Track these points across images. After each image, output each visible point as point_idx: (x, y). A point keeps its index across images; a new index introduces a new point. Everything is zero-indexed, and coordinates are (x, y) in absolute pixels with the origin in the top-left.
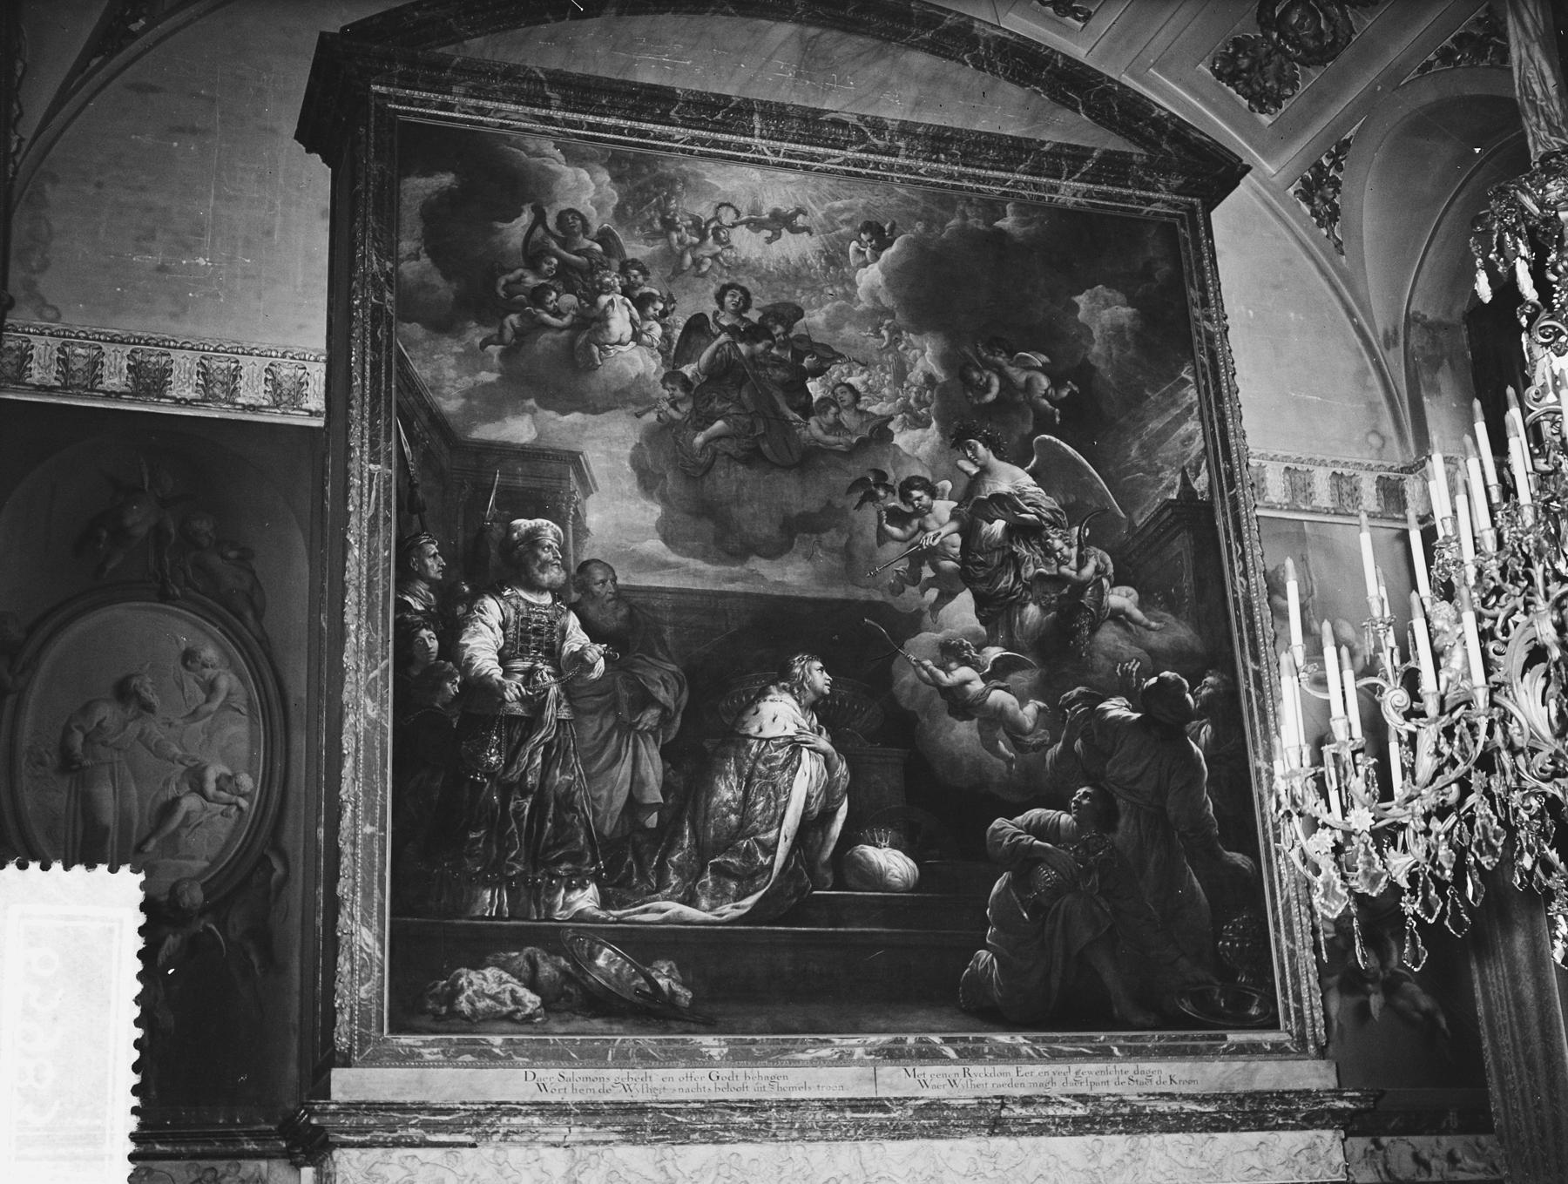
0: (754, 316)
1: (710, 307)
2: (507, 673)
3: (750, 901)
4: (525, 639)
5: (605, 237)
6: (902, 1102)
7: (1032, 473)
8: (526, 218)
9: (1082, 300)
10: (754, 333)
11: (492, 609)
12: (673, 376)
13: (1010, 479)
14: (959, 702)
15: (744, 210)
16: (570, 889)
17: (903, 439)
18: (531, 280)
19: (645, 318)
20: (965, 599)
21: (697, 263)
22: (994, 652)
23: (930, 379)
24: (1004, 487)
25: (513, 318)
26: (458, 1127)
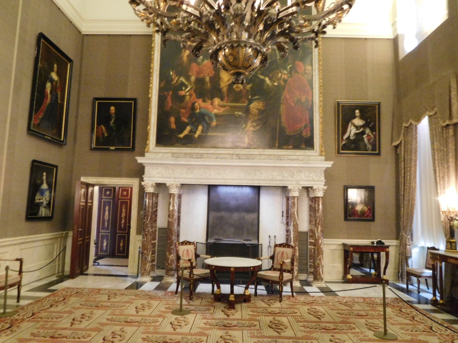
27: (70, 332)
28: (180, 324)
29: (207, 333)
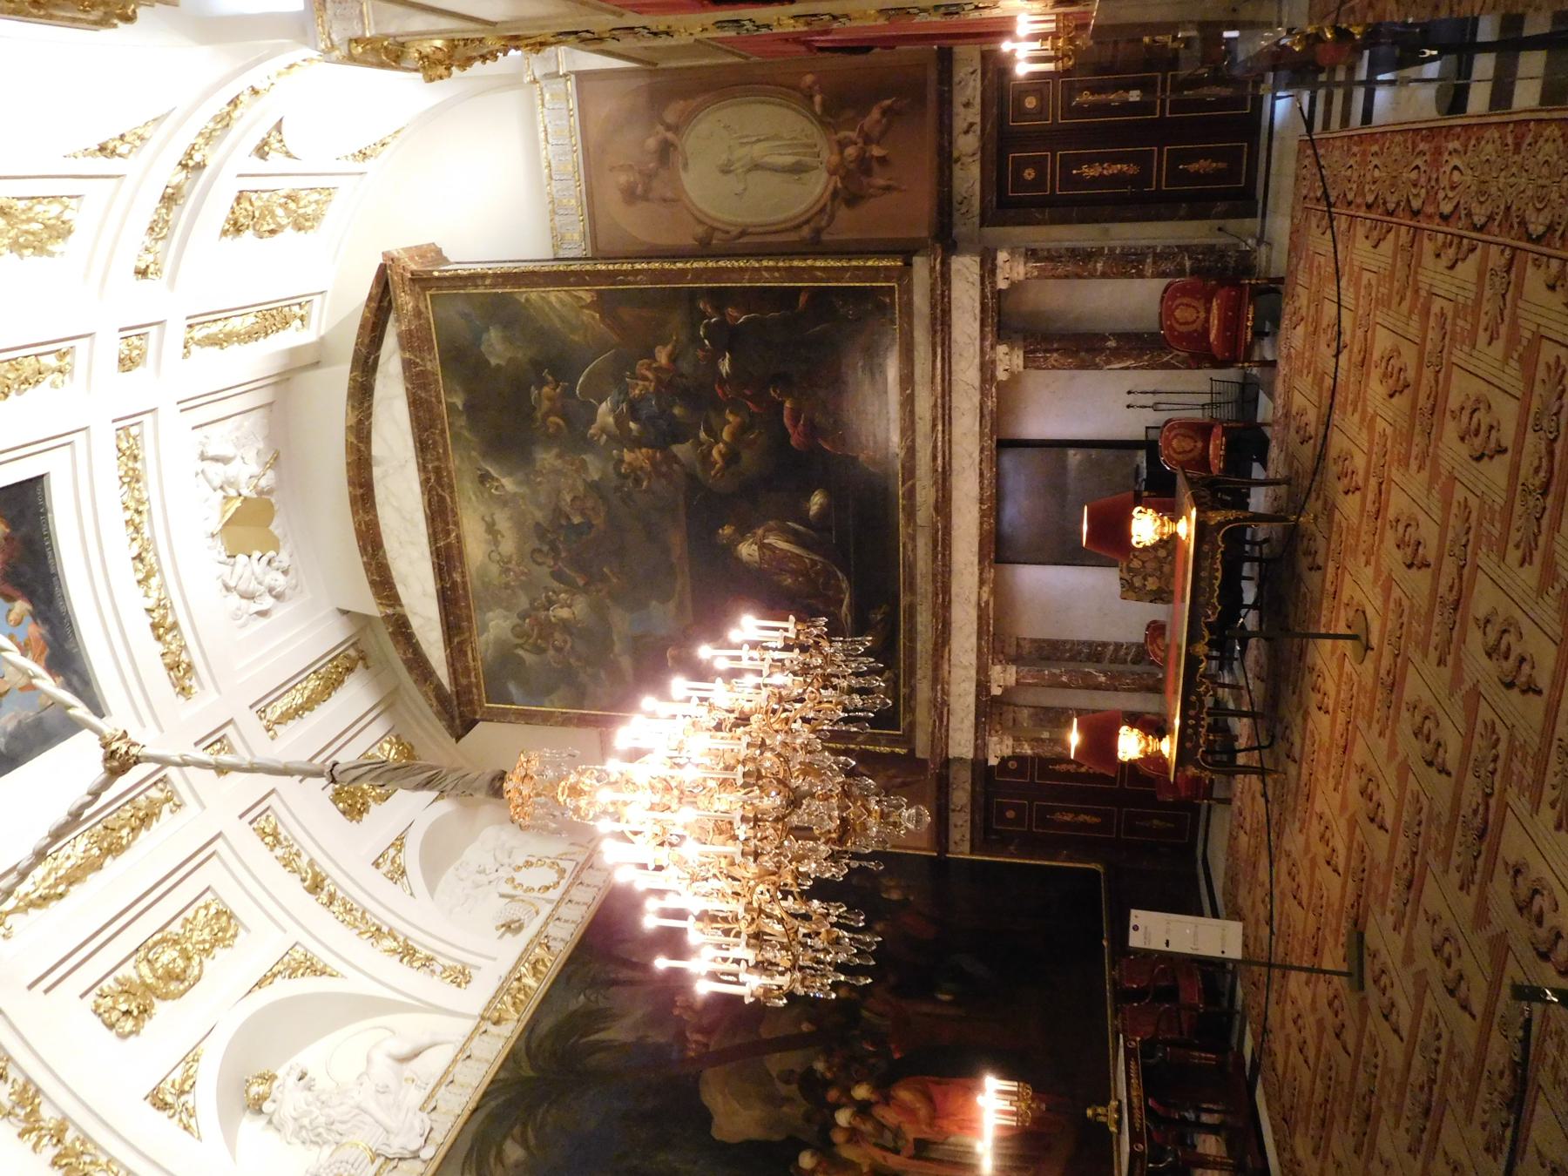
0: (545, 548)
1: (546, 570)
5: (523, 616)
8: (520, 652)
9: (493, 361)
14: (731, 457)
18: (551, 652)
21: (523, 573)
22: (702, 435)
24: (611, 420)
27: (1470, 778)
28: (1483, 428)
29: (1528, 335)
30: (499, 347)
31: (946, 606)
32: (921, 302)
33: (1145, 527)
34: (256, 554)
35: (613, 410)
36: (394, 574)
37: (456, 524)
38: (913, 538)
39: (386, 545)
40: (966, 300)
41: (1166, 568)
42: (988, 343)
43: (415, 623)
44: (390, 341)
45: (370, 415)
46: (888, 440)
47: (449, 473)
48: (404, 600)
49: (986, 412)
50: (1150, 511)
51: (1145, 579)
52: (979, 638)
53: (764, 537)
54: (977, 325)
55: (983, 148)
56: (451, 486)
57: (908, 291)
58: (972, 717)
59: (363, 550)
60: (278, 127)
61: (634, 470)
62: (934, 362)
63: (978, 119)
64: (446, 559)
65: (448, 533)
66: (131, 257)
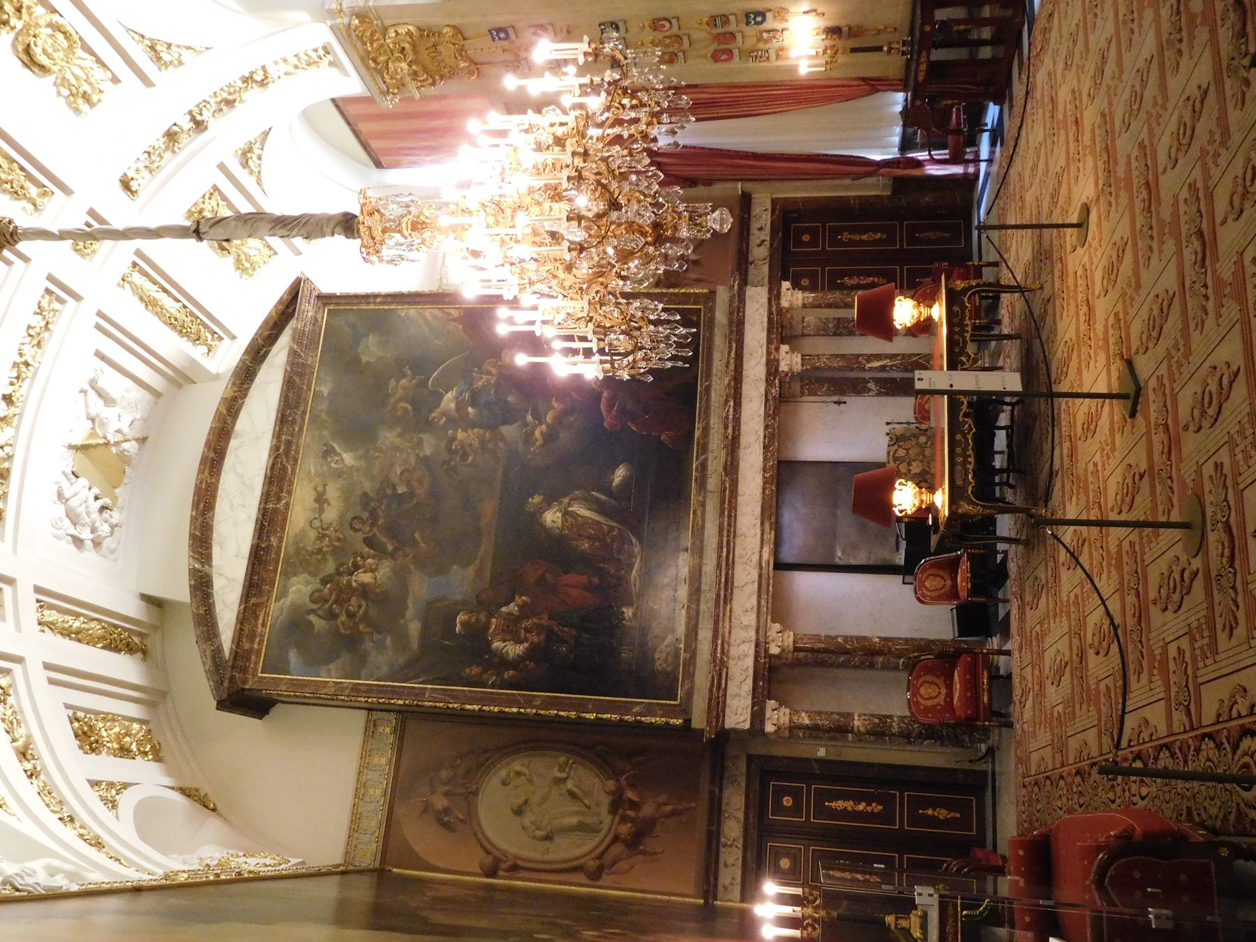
0: (365, 515)
1: (360, 536)
2: (526, 640)
3: (634, 540)
4: (511, 630)
5: (324, 582)
6: (723, 482)
7: (447, 392)
8: (312, 618)
9: (364, 359)
10: (374, 515)
11: (497, 645)
12: (392, 556)
13: (449, 401)
14: (550, 437)
15: (313, 516)
16: (624, 619)
17: (428, 451)
18: (343, 618)
19: (364, 566)
20: (504, 429)
21: (339, 540)
22: (529, 418)
23: (399, 435)
24: (453, 405)
25: (361, 627)
26: (720, 675)
30: (373, 349)
31: (733, 508)
32: (721, 316)
33: (904, 312)
34: (96, 491)
35: (456, 398)
36: (215, 535)
37: (290, 493)
38: (703, 505)
39: (218, 509)
40: (756, 316)
41: (927, 452)
42: (773, 347)
43: (218, 584)
44: (285, 340)
45: (245, 396)
46: (672, 619)
47: (298, 446)
48: (215, 562)
49: (770, 397)
50: (909, 483)
51: (909, 464)
52: (759, 596)
53: (569, 505)
54: (764, 334)
55: (771, 256)
56: (296, 460)
57: (712, 310)
58: (750, 681)
59: (196, 505)
60: (266, 134)
61: (463, 447)
62: (729, 352)
63: (768, 238)
64: (269, 521)
65: (279, 500)
66: (126, 163)
